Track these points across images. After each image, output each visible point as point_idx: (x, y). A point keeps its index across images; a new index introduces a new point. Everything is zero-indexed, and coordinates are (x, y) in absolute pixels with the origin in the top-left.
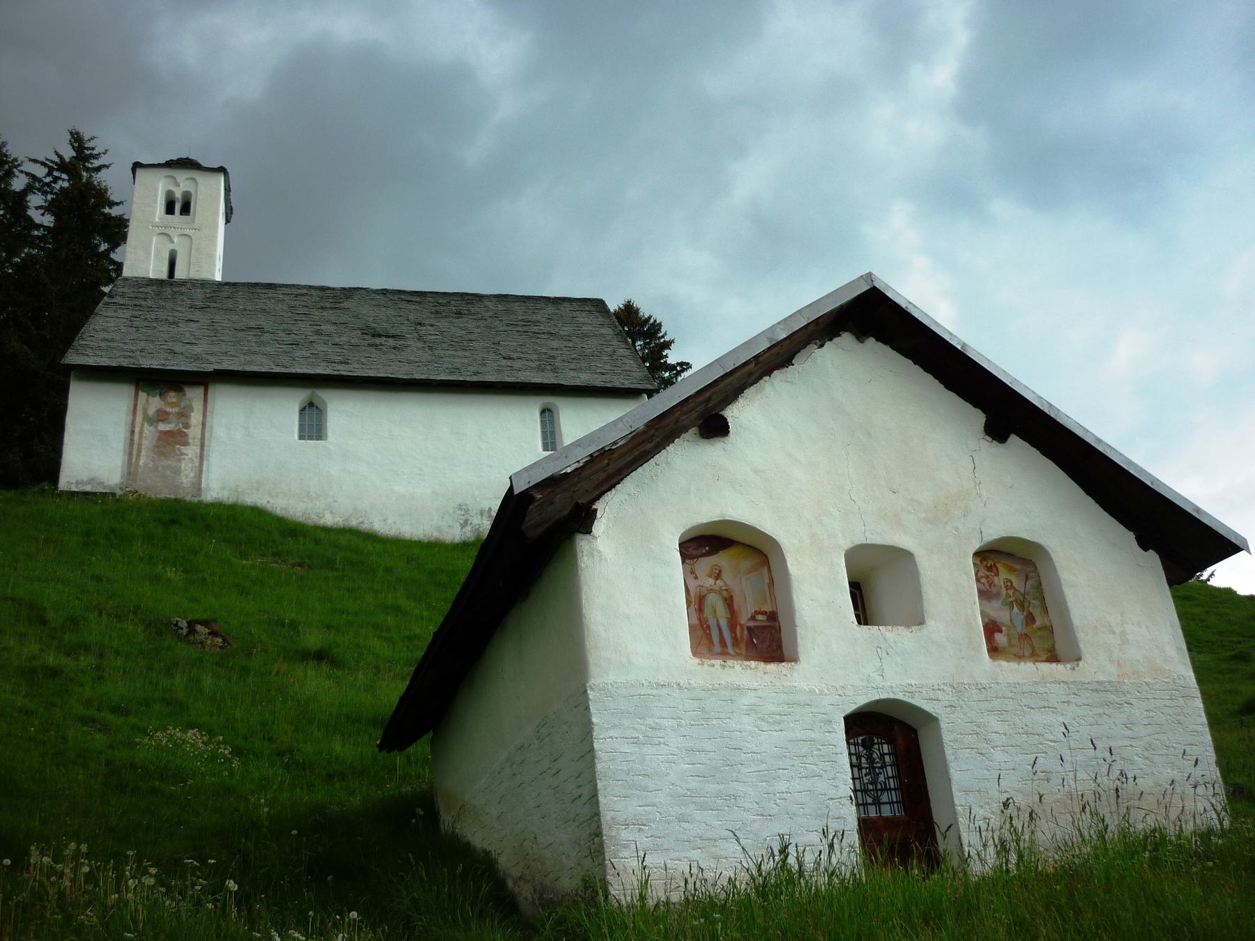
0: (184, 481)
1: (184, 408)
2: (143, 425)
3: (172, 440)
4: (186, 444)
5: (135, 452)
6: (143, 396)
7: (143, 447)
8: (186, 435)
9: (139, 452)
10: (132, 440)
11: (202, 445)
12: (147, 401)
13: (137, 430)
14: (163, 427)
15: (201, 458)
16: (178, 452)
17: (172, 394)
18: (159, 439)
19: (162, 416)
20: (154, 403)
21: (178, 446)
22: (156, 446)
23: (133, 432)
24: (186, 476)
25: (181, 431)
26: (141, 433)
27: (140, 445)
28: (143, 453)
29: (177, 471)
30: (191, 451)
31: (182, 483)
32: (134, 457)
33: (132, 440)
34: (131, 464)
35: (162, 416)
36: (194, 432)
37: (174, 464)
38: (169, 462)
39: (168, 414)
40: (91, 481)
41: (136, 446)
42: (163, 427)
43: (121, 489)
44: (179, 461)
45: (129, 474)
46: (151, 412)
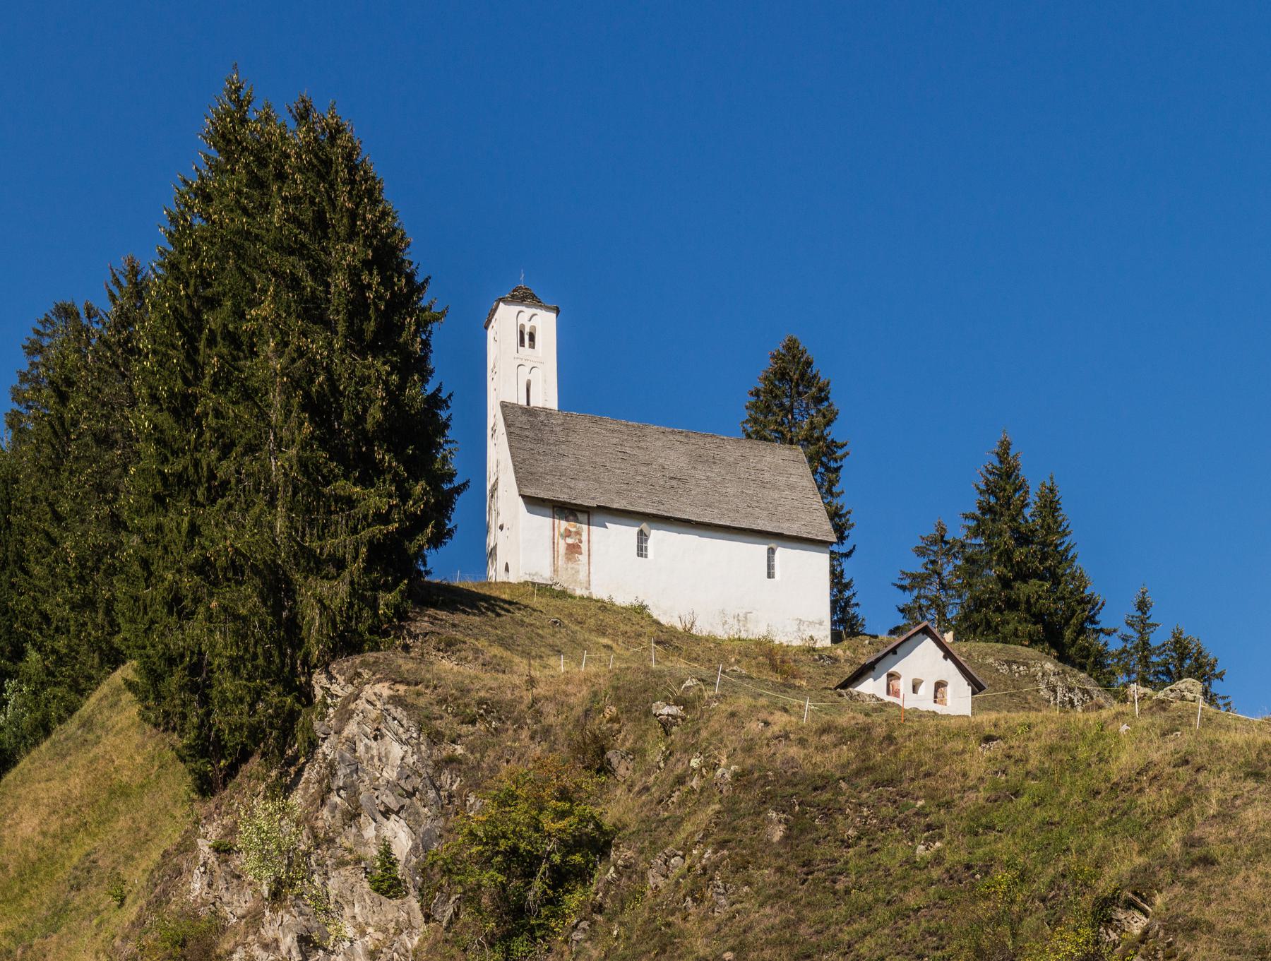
3: (573, 549)
4: (581, 553)
6: (557, 521)
8: (580, 547)
14: (570, 541)
17: (571, 518)
19: (568, 534)
20: (564, 525)
24: (582, 576)
30: (583, 558)
35: (568, 534)
36: (584, 546)
39: (570, 532)
40: (536, 574)
42: (570, 541)
46: (562, 530)
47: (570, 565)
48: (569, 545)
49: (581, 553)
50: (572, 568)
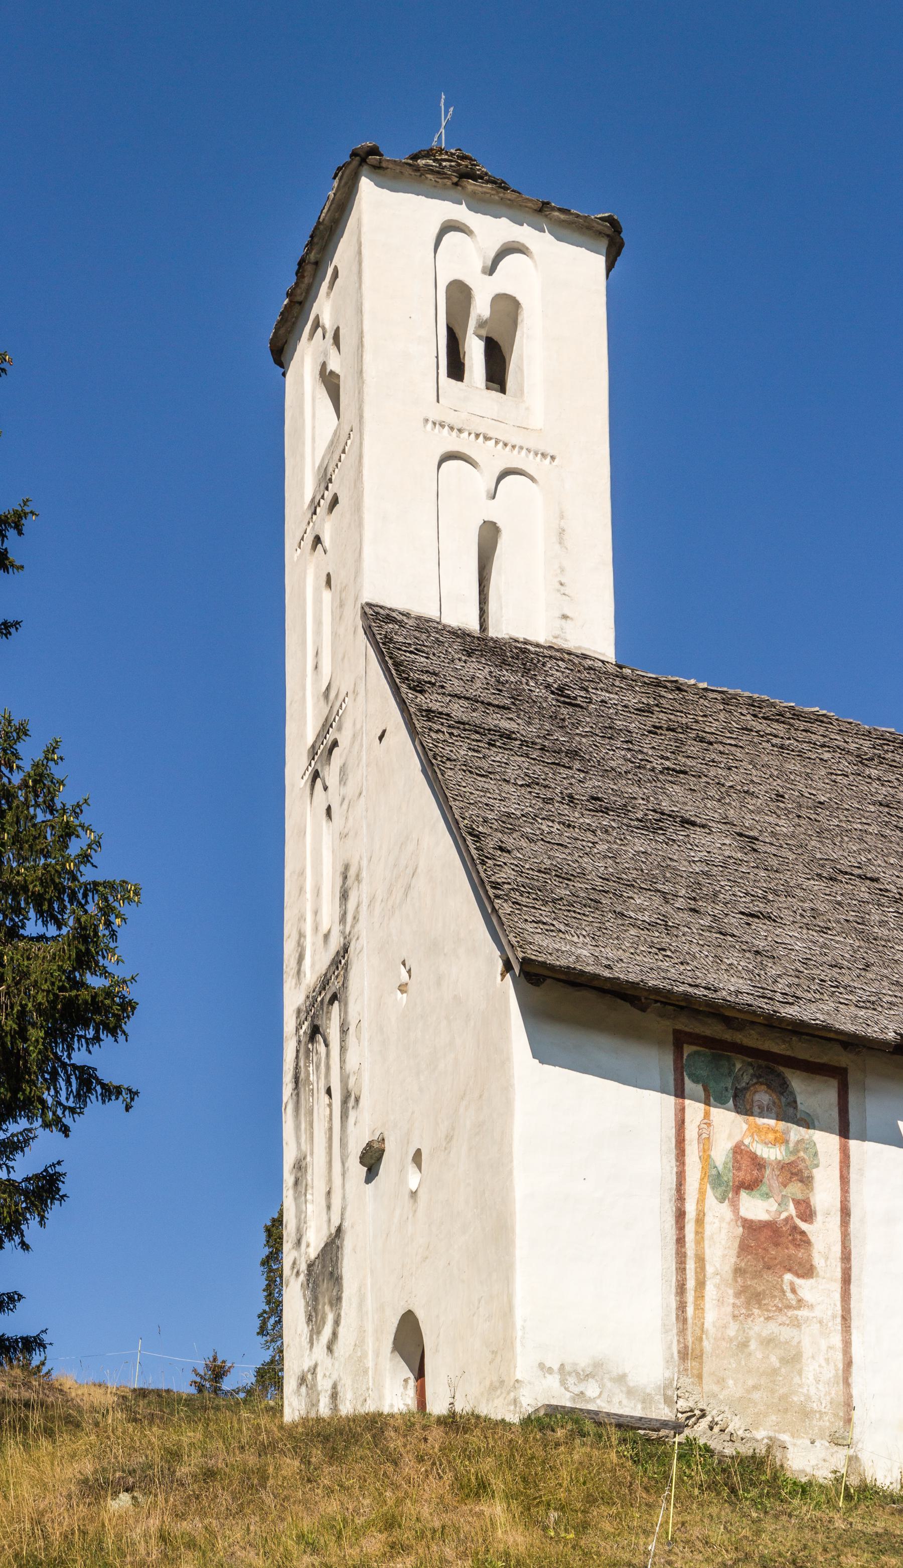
0: (813, 1391)
1: (796, 1151)
2: (701, 1200)
4: (807, 1271)
5: (691, 1284)
7: (710, 1269)
8: (802, 1240)
9: (701, 1284)
10: (680, 1241)
11: (846, 1280)
12: (707, 1115)
13: (691, 1208)
15: (846, 1317)
16: (789, 1295)
18: (744, 1248)
21: (788, 1277)
22: (738, 1271)
23: (680, 1215)
25: (795, 1228)
26: (700, 1221)
27: (701, 1260)
28: (710, 1290)
29: (793, 1359)
31: (808, 1397)
32: (690, 1296)
33: (680, 1241)
34: (685, 1321)
37: (786, 1333)
38: (772, 1328)
41: (691, 1265)
43: (668, 1401)
44: (796, 1324)
45: (684, 1354)
47: (759, 1327)
48: (751, 1228)
49: (807, 1271)
50: (768, 1342)
